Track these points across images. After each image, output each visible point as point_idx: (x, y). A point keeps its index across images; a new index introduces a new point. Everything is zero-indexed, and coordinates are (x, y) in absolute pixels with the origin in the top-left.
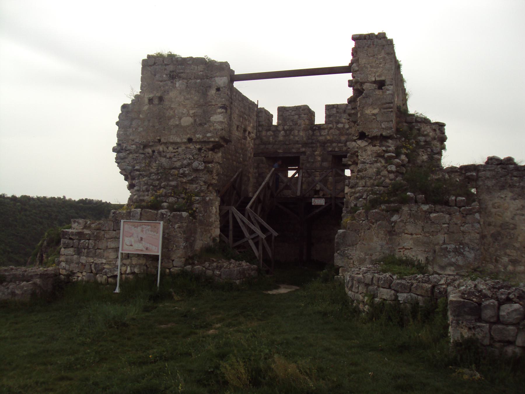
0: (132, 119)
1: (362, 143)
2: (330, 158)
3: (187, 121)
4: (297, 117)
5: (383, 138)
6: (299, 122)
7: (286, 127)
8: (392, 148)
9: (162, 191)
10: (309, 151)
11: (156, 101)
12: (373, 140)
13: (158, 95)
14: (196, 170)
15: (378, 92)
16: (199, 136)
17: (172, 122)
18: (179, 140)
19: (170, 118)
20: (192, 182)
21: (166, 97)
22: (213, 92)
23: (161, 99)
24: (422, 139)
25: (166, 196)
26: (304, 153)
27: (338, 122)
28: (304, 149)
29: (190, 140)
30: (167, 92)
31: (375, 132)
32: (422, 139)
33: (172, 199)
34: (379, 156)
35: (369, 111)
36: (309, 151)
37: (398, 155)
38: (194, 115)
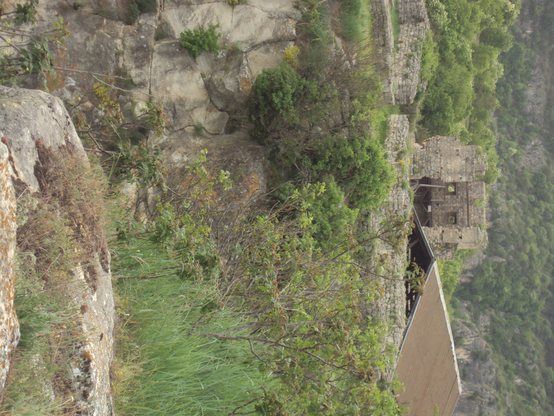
0: (450, 143)
1: (441, 231)
2: (455, 211)
3: (449, 166)
4: (478, 192)
5: (442, 239)
6: (475, 194)
7: (472, 187)
8: (439, 242)
9: (420, 162)
10: (459, 200)
11: (457, 153)
12: (441, 235)
13: (460, 154)
14: (430, 172)
15: (458, 237)
16: (443, 172)
17: (449, 160)
18: (442, 163)
19: (450, 159)
20: (425, 171)
21: (459, 157)
22: (460, 176)
23: (458, 155)
24: (445, 252)
25: (419, 165)
26: (458, 198)
27: (474, 214)
28: (459, 197)
29: (442, 168)
30: (461, 158)
31: (444, 236)
32: (445, 252)
33: (417, 167)
34: (436, 238)
35: (451, 234)
36: (459, 200)
37: (437, 244)
38: (451, 169)
